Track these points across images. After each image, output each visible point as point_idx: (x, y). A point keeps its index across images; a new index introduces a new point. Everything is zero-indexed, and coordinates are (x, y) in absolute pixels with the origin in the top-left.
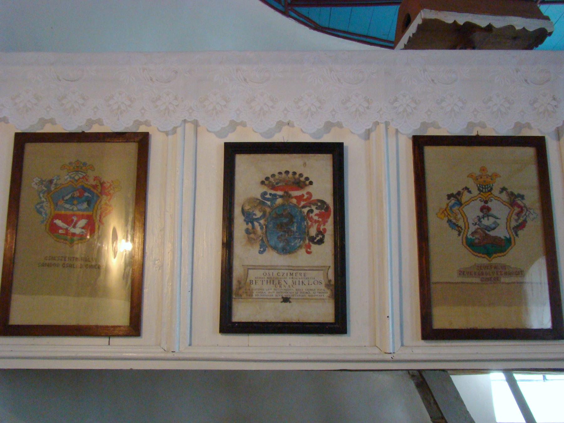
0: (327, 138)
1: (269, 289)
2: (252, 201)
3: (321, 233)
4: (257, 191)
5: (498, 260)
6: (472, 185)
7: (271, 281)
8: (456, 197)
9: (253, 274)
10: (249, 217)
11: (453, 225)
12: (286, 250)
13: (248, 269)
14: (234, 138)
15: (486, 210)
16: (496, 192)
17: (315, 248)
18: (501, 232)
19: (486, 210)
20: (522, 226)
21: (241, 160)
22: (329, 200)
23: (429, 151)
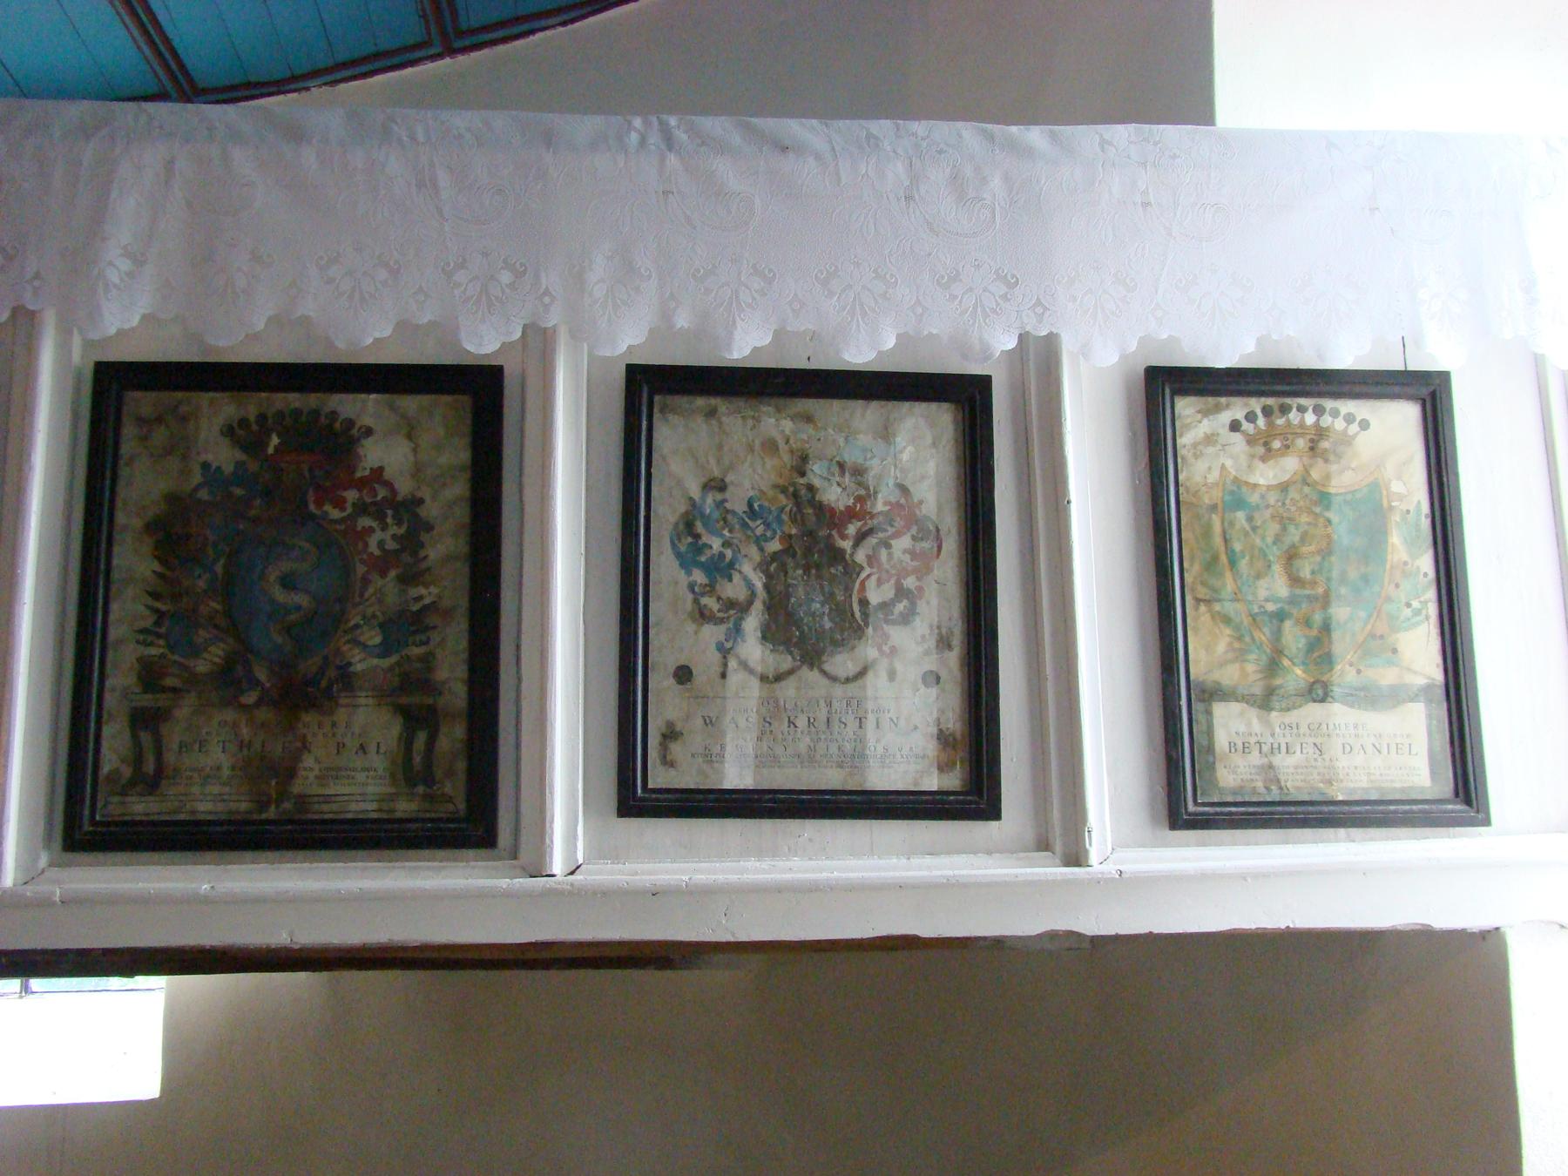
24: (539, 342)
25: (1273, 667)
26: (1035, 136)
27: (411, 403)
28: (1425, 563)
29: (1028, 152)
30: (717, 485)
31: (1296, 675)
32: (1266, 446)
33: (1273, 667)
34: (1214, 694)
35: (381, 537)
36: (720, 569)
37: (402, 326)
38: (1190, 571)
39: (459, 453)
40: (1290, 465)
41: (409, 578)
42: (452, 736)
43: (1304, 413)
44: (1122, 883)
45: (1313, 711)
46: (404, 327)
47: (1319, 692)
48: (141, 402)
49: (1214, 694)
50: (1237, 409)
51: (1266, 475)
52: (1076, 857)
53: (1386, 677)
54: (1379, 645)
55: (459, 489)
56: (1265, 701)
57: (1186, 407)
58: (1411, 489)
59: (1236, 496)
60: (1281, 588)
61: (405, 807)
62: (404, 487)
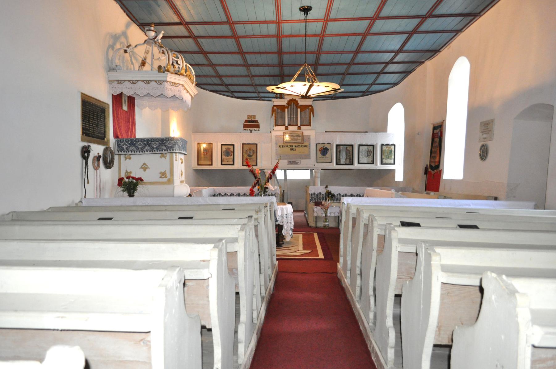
0: (232, 144)
1: (226, 161)
2: (224, 151)
3: (232, 154)
4: (225, 150)
5: (251, 157)
6: (249, 149)
7: (227, 160)
8: (247, 151)
9: (224, 159)
10: (224, 153)
11: (246, 153)
12: (228, 156)
13: (224, 158)
14: (222, 143)
15: (250, 152)
16: (251, 150)
17: (231, 156)
18: (251, 154)
19: (250, 152)
20: (254, 154)
21: (223, 146)
22: (232, 151)
23: (244, 145)
24: (355, 144)
25: (386, 158)
26: (377, 133)
27: (350, 146)
28: (394, 153)
29: (376, 134)
30: (362, 150)
31: (387, 158)
32: (387, 148)
33: (386, 158)
34: (383, 159)
35: (348, 152)
36: (362, 153)
37: (349, 143)
38: (383, 153)
39: (351, 148)
40: (388, 149)
41: (350, 154)
42: (351, 161)
43: (389, 146)
44: (379, 167)
45: (388, 160)
46: (349, 143)
47: (388, 159)
48: (338, 146)
49: (383, 159)
50: (385, 146)
51: (387, 149)
52: (377, 166)
53: (391, 158)
54: (391, 157)
55: (352, 150)
56: (386, 159)
57: (383, 146)
58: (393, 150)
59: (385, 150)
60: (387, 154)
61: (350, 163)
62: (349, 150)
